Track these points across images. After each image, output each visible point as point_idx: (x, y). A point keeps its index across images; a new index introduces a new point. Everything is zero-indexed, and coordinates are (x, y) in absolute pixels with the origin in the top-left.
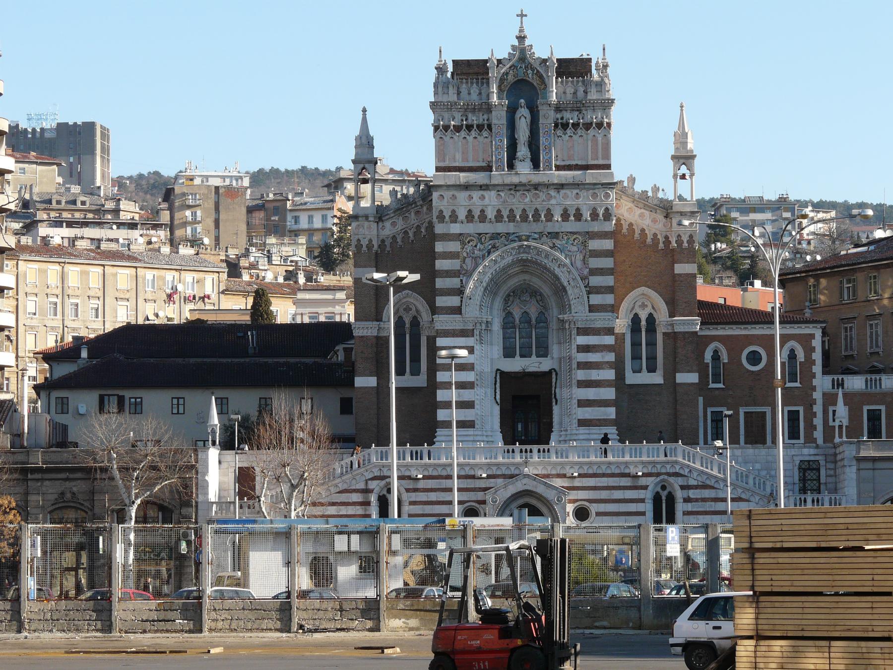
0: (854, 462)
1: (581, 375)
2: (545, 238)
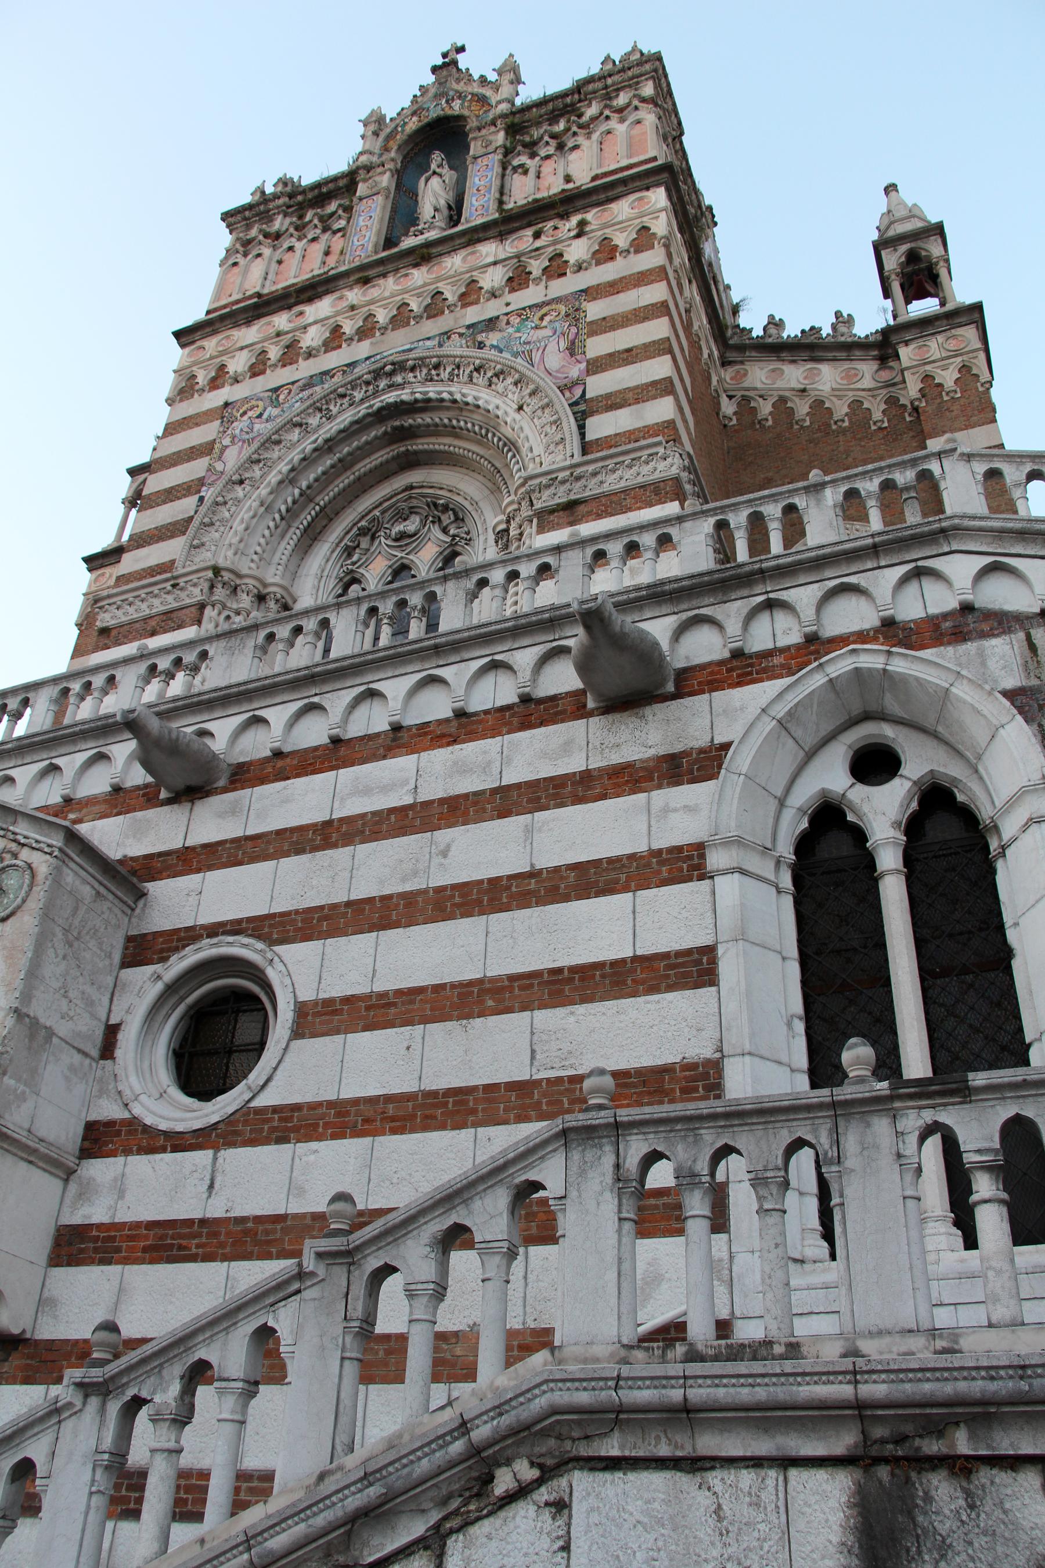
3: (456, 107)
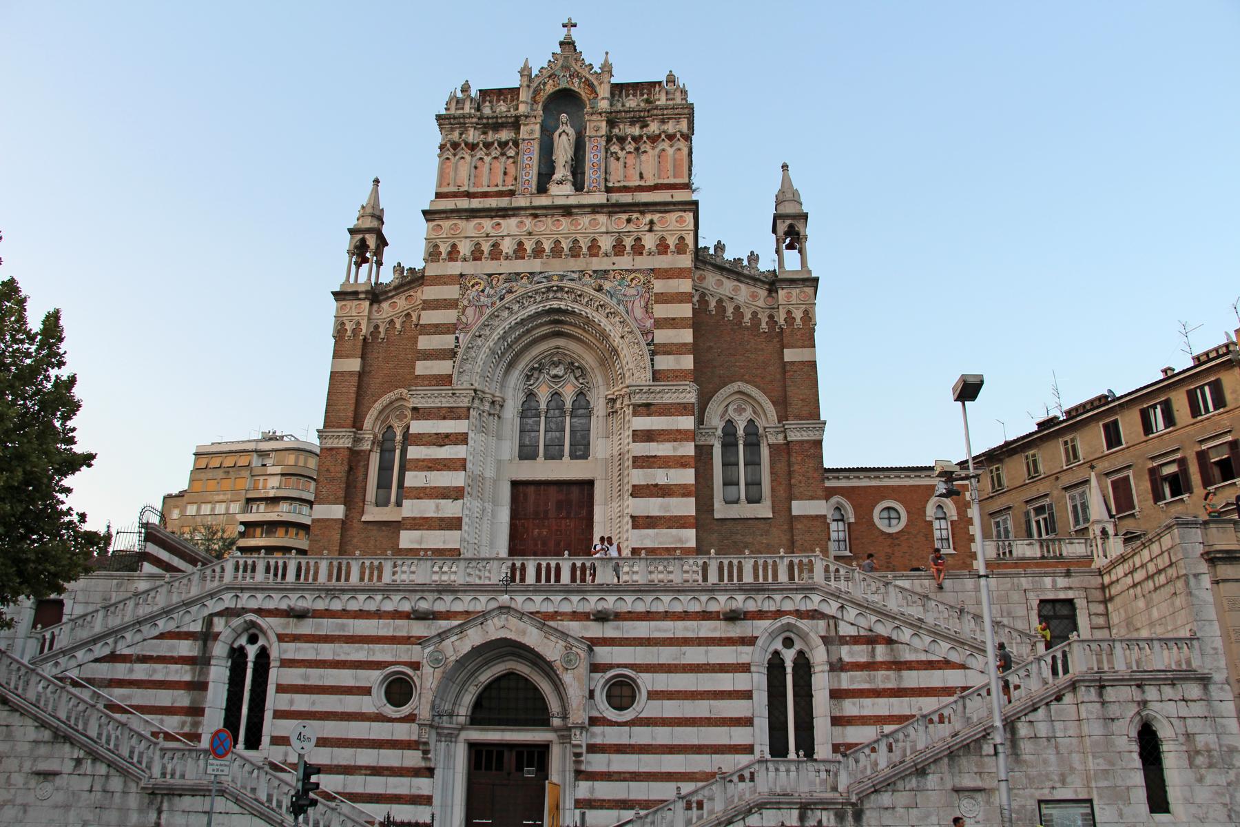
0: (1203, 567)
1: (639, 477)
2: (587, 279)
3: (576, 86)
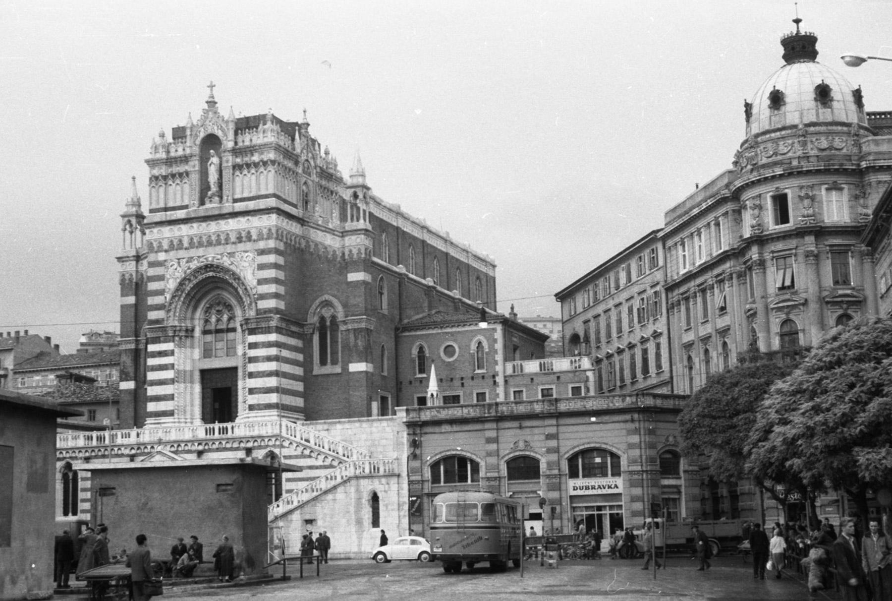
2: (225, 258)
